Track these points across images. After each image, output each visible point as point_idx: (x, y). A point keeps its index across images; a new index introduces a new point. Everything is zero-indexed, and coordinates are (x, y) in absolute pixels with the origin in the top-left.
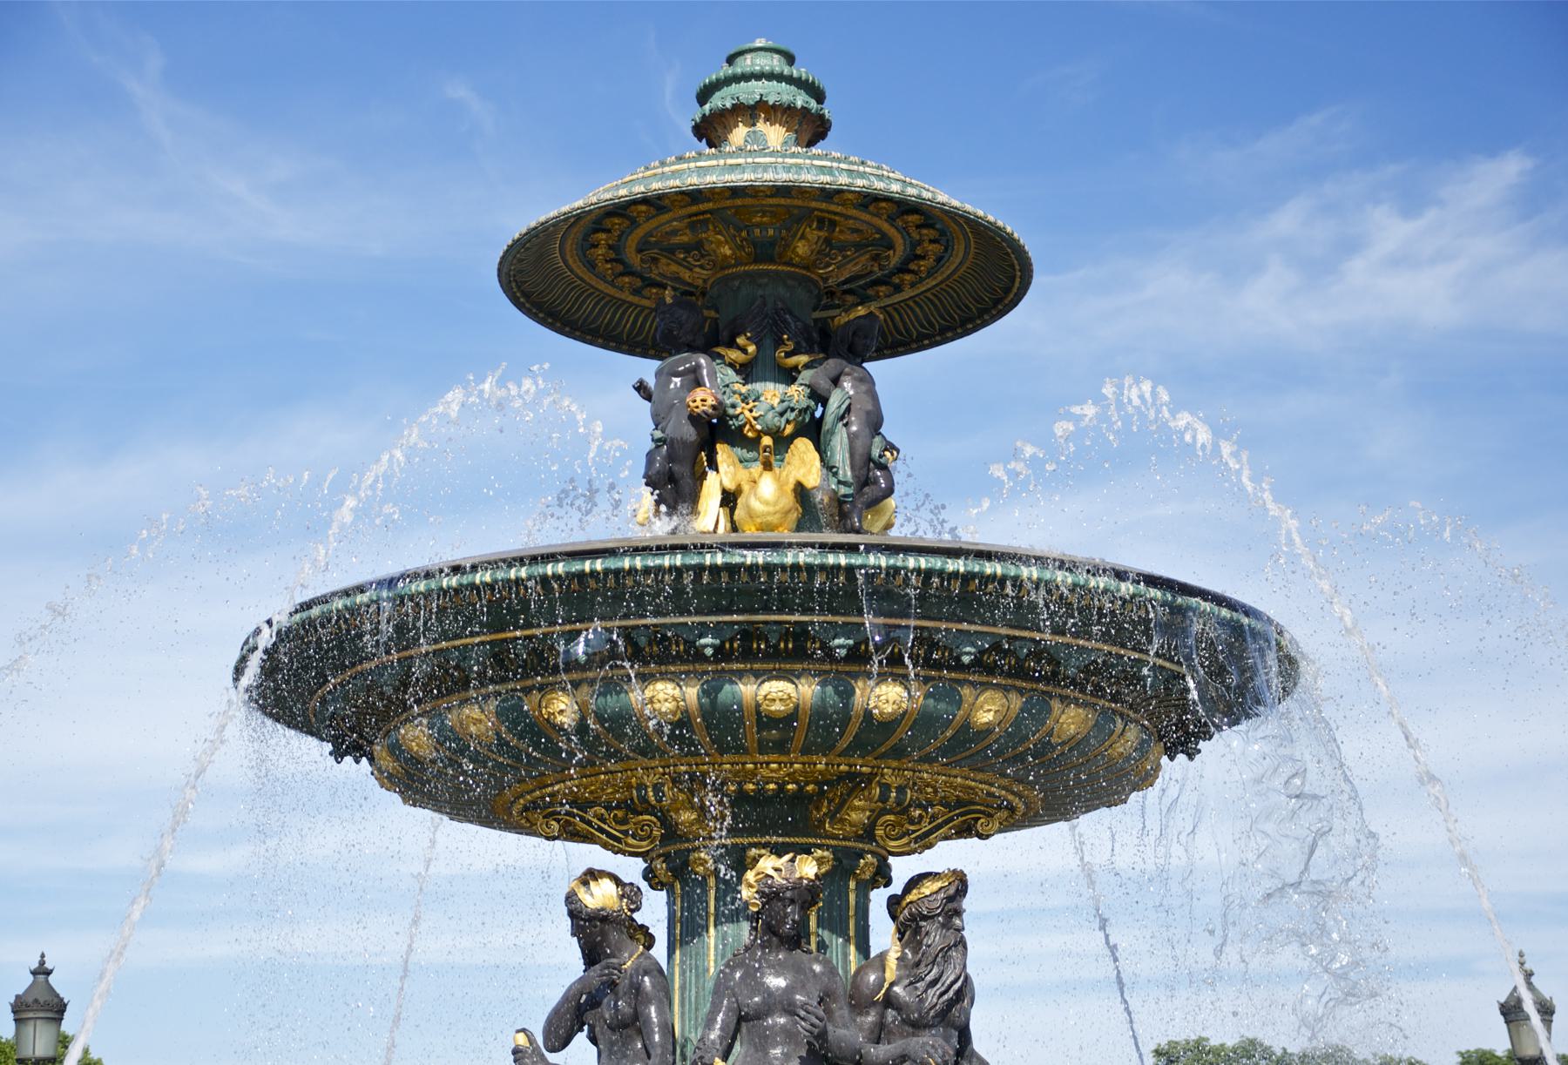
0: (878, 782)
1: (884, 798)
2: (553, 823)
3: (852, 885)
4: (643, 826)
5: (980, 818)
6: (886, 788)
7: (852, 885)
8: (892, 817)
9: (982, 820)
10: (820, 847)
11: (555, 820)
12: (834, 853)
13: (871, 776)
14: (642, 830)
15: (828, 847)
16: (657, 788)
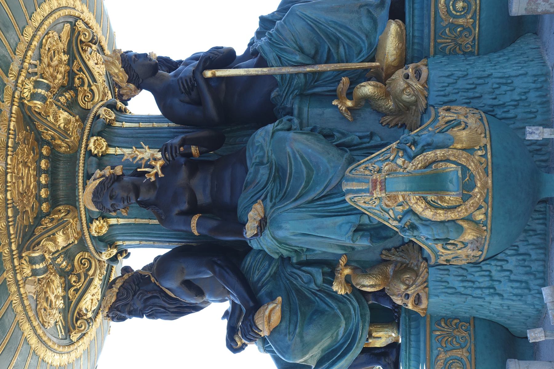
0: (28, 101)
1: (44, 99)
2: (79, 322)
3: (118, 124)
5: (81, 40)
6: (34, 96)
7: (118, 124)
8: (80, 97)
9: (83, 39)
10: (87, 145)
11: (77, 321)
12: (93, 136)
13: (22, 105)
14: (85, 264)
15: (88, 140)
16: (32, 261)
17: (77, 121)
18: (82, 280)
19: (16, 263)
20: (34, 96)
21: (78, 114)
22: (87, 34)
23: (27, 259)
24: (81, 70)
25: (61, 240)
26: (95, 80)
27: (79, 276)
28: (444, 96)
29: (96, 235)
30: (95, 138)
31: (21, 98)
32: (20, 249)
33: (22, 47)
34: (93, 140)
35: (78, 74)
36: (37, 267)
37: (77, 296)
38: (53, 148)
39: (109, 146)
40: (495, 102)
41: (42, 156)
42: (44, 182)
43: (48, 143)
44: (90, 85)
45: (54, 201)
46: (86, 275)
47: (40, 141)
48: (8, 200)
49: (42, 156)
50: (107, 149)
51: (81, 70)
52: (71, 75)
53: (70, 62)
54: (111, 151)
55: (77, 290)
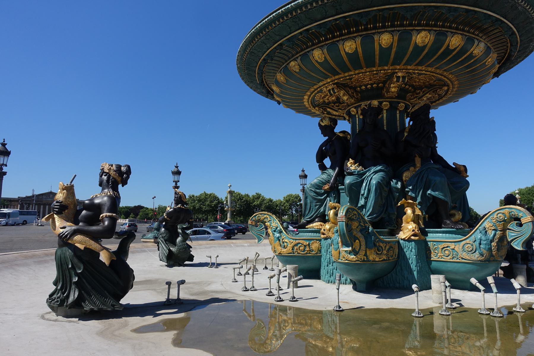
2: (321, 109)
3: (398, 112)
4: (343, 106)
5: (437, 90)
7: (398, 112)
8: (411, 94)
10: (385, 101)
11: (322, 108)
12: (390, 103)
15: (387, 101)
17: (395, 95)
18: (337, 108)
19: (331, 83)
20: (398, 78)
21: (398, 95)
22: (441, 92)
23: (334, 87)
24: (423, 92)
25: (345, 98)
27: (338, 106)
29: (351, 110)
30: (388, 104)
31: (397, 73)
32: (336, 84)
35: (421, 91)
36: (331, 91)
37: (331, 107)
38: (382, 88)
39: (387, 110)
41: (378, 84)
42: (368, 87)
43: (384, 86)
44: (416, 97)
45: (362, 91)
46: (339, 109)
47: (384, 83)
48: (352, 76)
49: (378, 84)
50: (385, 109)
51: (423, 92)
53: (426, 87)
54: (385, 112)
55: (333, 106)
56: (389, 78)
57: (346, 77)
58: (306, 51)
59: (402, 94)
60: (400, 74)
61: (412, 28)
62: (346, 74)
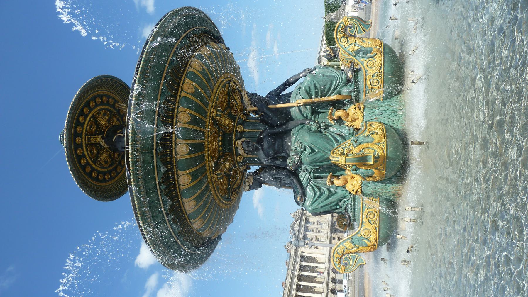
1: (220, 116)
16: (218, 175)
20: (217, 115)
26: (237, 104)
28: (370, 117)
33: (212, 97)
34: (238, 127)
37: (233, 184)
38: (224, 132)
40: (389, 120)
52: (228, 103)
56: (215, 122)
57: (209, 160)
58: (178, 192)
59: (232, 118)
60: (215, 113)
61: (178, 96)
62: (207, 159)
